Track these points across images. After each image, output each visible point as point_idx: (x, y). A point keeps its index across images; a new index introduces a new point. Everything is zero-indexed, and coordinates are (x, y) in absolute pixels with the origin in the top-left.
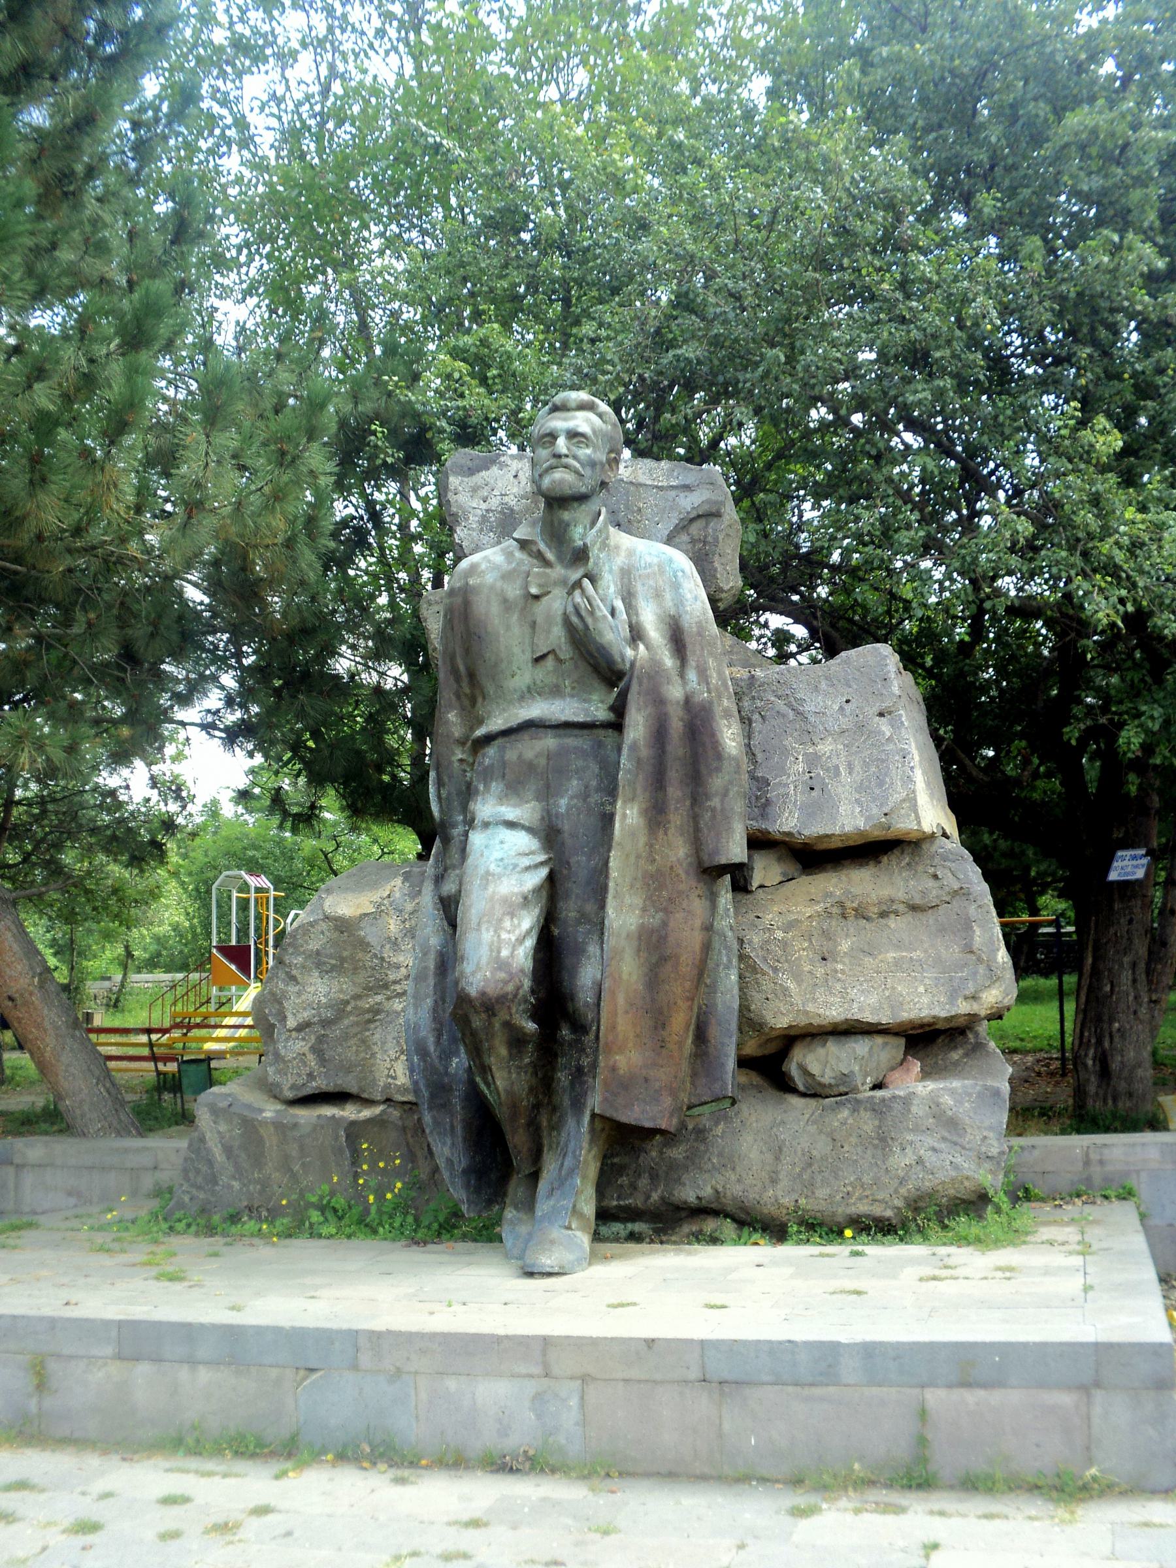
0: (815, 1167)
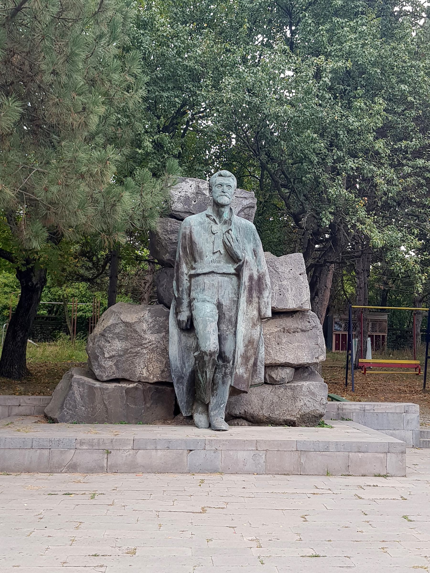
0: (274, 405)
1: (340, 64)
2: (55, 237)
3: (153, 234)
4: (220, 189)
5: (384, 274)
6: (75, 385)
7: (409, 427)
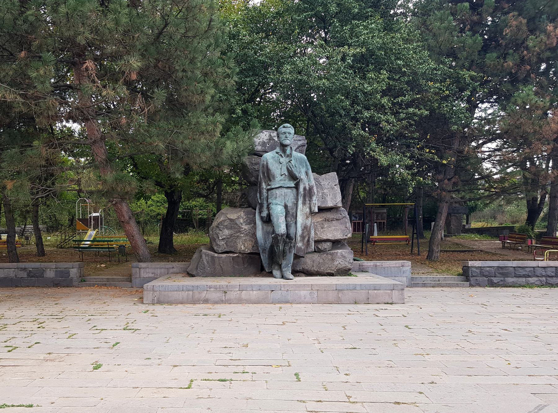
1: (358, 50)
2: (187, 170)
3: (244, 166)
4: (284, 136)
5: (384, 184)
6: (204, 256)
7: (404, 275)
